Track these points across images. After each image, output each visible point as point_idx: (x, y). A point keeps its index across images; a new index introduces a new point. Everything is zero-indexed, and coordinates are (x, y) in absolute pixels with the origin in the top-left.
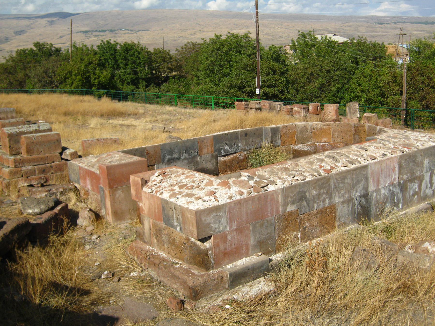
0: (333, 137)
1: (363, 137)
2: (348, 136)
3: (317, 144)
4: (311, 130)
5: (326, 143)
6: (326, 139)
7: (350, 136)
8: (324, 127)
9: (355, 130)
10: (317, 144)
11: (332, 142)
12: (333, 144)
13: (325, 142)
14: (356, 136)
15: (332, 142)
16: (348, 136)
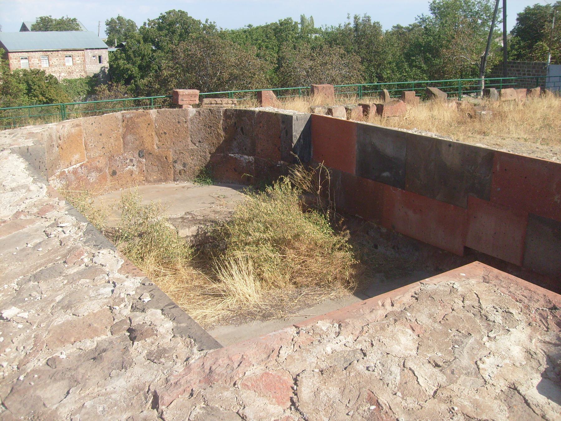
0: (86, 149)
1: (145, 135)
2: (112, 140)
3: (66, 170)
4: (57, 141)
5: (78, 165)
6: (77, 157)
7: (117, 139)
8: (73, 130)
9: (127, 127)
10: (66, 170)
11: (87, 160)
12: (89, 164)
13: (77, 162)
14: (129, 137)
15: (87, 160)
16: (112, 140)
